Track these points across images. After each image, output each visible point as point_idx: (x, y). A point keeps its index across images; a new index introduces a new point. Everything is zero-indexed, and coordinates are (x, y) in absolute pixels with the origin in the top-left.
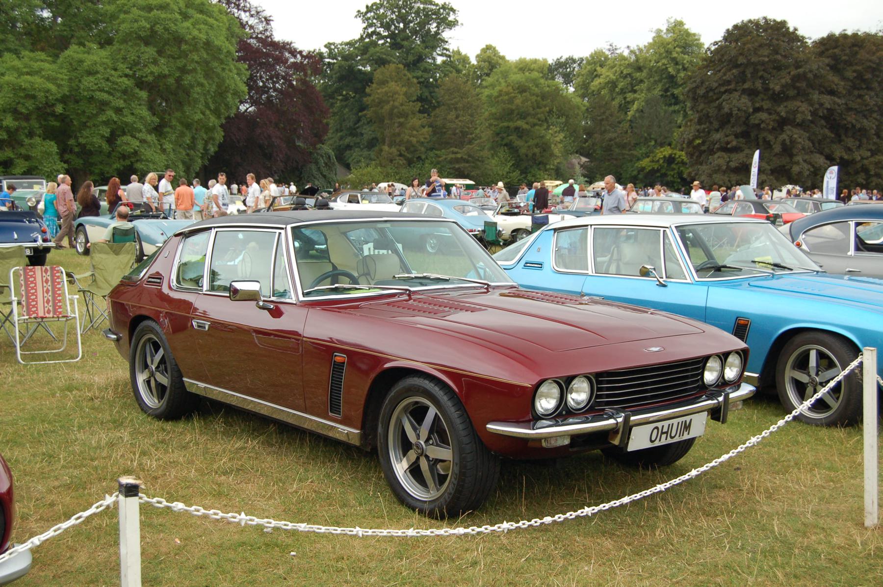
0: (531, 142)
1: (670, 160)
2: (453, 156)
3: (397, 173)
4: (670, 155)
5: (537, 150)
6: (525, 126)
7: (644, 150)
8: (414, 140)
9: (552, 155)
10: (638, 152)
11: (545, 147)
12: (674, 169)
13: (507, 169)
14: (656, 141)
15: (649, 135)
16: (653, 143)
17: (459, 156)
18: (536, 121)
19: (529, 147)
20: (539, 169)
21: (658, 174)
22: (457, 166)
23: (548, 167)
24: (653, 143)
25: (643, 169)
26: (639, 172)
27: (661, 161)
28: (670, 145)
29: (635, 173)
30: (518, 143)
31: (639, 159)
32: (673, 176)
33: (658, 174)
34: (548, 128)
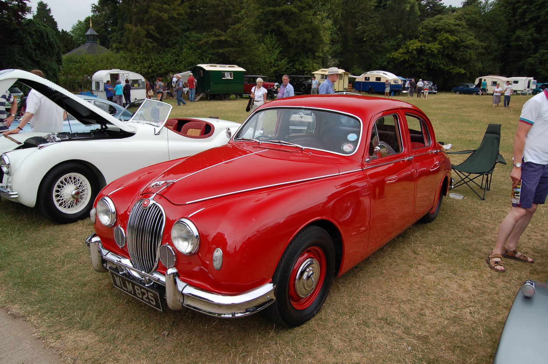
0: (302, 27)
1: (421, 51)
2: (216, 39)
3: (147, 60)
4: (421, 46)
5: (309, 36)
6: (294, 10)
7: (393, 42)
8: (165, 16)
9: (321, 41)
10: (386, 44)
11: (315, 32)
12: (423, 60)
13: (275, 57)
14: (403, 34)
15: (397, 29)
16: (401, 36)
17: (223, 38)
18: (304, 5)
19: (299, 32)
20: (308, 58)
21: (406, 65)
22: (221, 51)
23: (317, 54)
24: (401, 36)
25: (394, 59)
26: (389, 63)
27: (415, 52)
28: (417, 37)
29: (385, 63)
30: (287, 28)
31: (388, 51)
32: (421, 67)
33: (406, 65)
34: (315, 14)
